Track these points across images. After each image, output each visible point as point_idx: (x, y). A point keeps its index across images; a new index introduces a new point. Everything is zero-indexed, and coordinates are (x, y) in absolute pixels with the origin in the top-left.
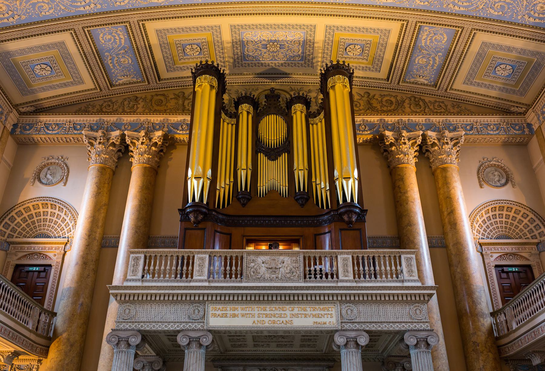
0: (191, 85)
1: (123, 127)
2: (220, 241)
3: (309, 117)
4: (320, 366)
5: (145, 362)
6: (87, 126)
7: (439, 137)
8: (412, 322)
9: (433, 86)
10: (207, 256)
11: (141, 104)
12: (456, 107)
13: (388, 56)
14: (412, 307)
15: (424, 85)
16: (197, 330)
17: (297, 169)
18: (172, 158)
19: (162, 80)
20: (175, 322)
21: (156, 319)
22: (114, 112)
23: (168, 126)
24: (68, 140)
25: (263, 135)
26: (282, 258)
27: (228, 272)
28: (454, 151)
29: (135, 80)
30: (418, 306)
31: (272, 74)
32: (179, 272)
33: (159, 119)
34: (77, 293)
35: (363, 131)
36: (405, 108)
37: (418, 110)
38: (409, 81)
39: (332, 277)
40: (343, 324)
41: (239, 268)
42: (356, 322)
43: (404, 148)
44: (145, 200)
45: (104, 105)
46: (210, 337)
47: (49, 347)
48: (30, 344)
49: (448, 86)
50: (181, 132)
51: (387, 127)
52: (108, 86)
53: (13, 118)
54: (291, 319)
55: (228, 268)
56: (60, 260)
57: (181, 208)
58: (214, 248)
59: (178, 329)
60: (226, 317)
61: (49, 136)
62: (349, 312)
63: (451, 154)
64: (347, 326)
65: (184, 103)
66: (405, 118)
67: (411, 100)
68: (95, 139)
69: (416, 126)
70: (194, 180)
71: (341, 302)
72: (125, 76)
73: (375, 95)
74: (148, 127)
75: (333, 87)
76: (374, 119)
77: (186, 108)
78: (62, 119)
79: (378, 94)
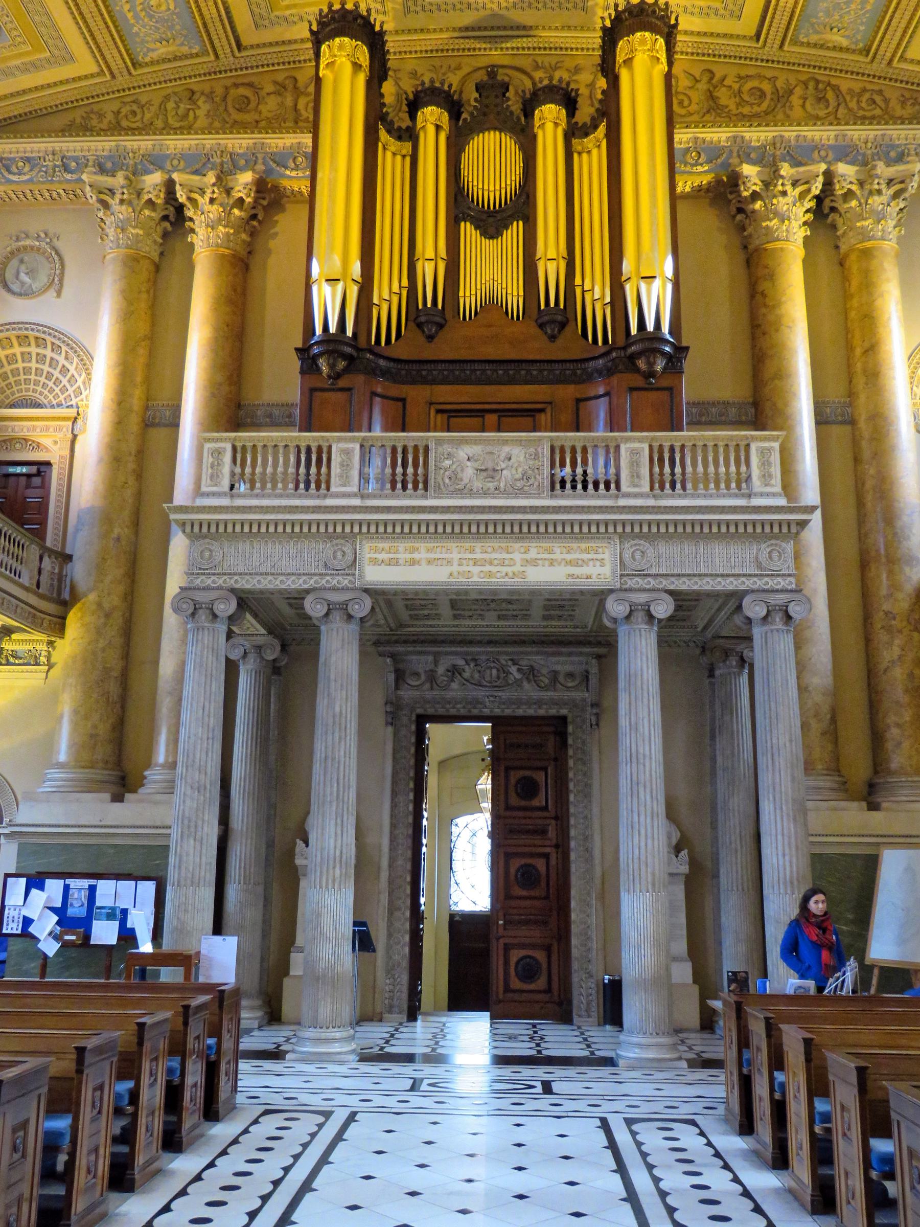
0: (310, 60)
1: (168, 163)
2: (384, 412)
3: (573, 135)
4: (581, 654)
5: (248, 645)
6: (90, 163)
7: (862, 177)
8: (761, 575)
9: (860, 52)
10: (358, 446)
11: (204, 107)
12: (909, 103)
14: (763, 546)
15: (841, 49)
16: (343, 589)
17: (543, 259)
18: (276, 234)
19: (246, 48)
20: (300, 574)
21: (262, 570)
22: (146, 129)
23: (264, 158)
24: (55, 195)
25: (470, 179)
26: (506, 449)
27: (399, 478)
29: (185, 50)
30: (776, 545)
31: (492, 28)
32: (302, 478)
33: (245, 143)
34: (106, 517)
35: (693, 165)
36: (791, 108)
37: (822, 113)
38: (805, 40)
39: (607, 488)
40: (625, 579)
41: (420, 470)
42: (649, 575)
43: (782, 204)
44: (226, 329)
45: (124, 111)
46: (368, 602)
47: (64, 618)
48: (30, 613)
49: (895, 52)
50: (294, 174)
51: (746, 153)
52: (127, 67)
54: (523, 569)
55: (399, 470)
56: (67, 453)
57: (300, 345)
58: (370, 431)
59: (306, 586)
60: (397, 564)
61: (14, 187)
62: (638, 555)
63: (884, 217)
64: (631, 583)
65: (296, 105)
66: (790, 133)
67: (807, 88)
68: (112, 192)
69: (813, 151)
71: (623, 536)
72: (164, 42)
73: (724, 78)
74: (222, 164)
75: (628, 62)
76: (719, 135)
77: (301, 115)
78: (36, 146)
79: (732, 72)
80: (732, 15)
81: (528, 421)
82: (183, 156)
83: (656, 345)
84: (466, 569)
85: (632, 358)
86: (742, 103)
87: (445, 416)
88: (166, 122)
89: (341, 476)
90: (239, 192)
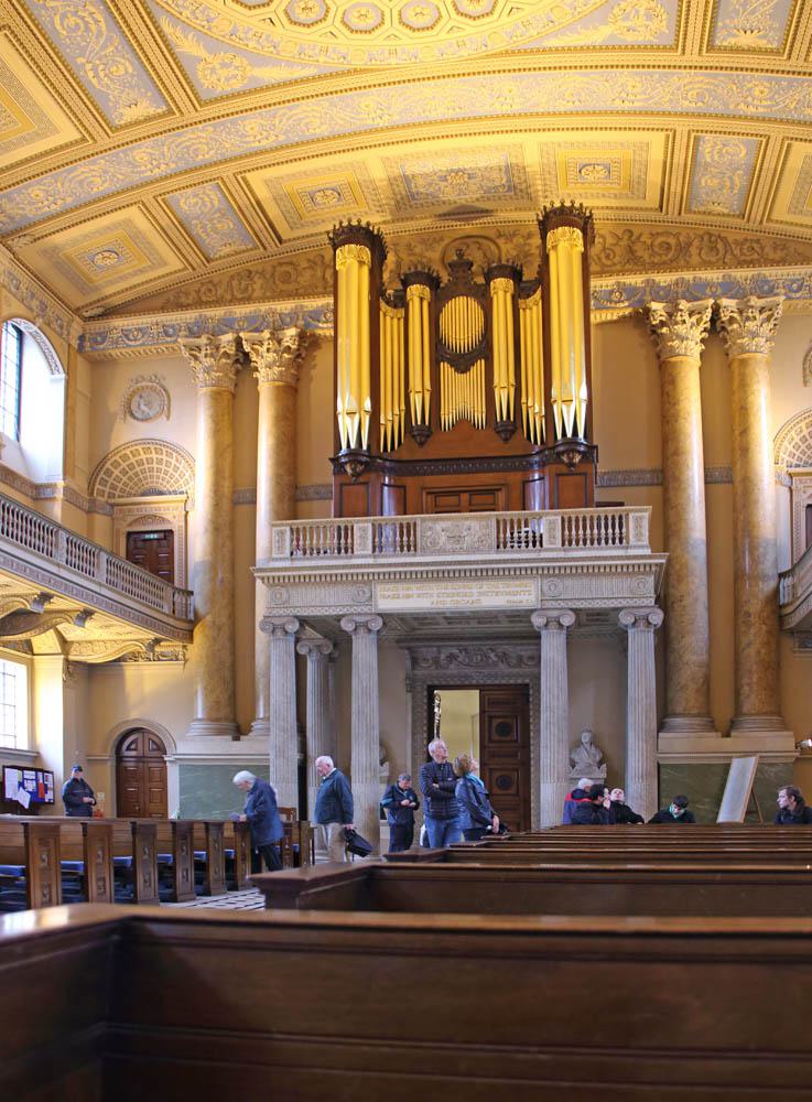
3: (520, 297)
7: (741, 307)
9: (738, 216)
10: (370, 525)
11: (259, 282)
13: (654, 176)
15: (724, 215)
18: (315, 365)
19: (285, 242)
21: (313, 604)
22: (218, 302)
26: (467, 523)
28: (768, 326)
29: (243, 247)
35: (616, 303)
36: (690, 256)
37: (713, 259)
41: (412, 538)
43: (680, 329)
45: (203, 290)
49: (763, 214)
50: (325, 325)
51: (658, 293)
53: (77, 327)
57: (332, 456)
58: (382, 515)
60: (398, 598)
63: (758, 336)
64: (548, 605)
66: (688, 276)
70: (347, 418)
71: (542, 576)
73: (641, 235)
74: (274, 322)
76: (636, 280)
80: (638, 198)
81: (487, 499)
82: (246, 318)
83: (572, 446)
84: (442, 599)
85: (559, 454)
86: (654, 254)
87: (433, 496)
88: (233, 295)
89: (360, 544)
90: (287, 342)
